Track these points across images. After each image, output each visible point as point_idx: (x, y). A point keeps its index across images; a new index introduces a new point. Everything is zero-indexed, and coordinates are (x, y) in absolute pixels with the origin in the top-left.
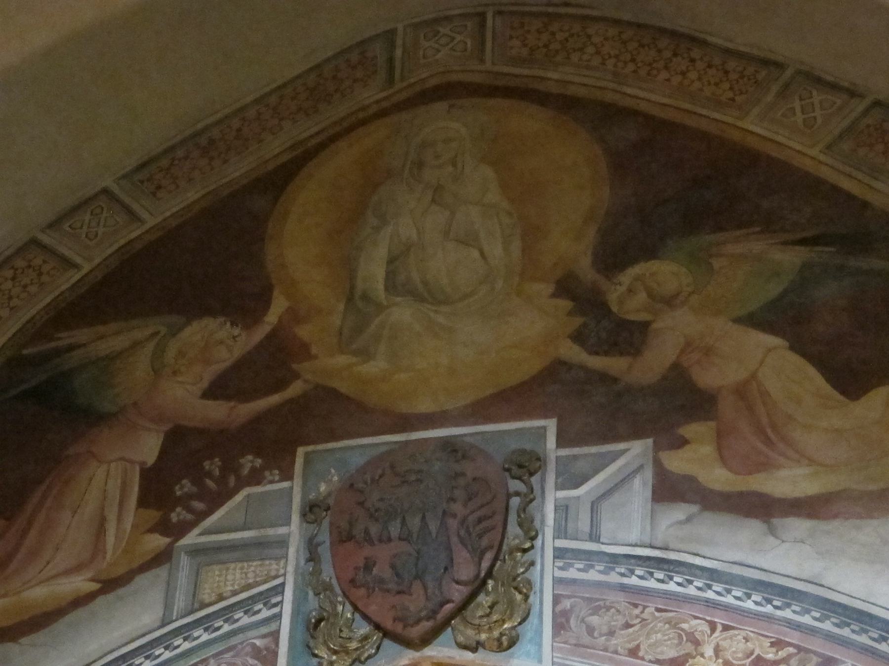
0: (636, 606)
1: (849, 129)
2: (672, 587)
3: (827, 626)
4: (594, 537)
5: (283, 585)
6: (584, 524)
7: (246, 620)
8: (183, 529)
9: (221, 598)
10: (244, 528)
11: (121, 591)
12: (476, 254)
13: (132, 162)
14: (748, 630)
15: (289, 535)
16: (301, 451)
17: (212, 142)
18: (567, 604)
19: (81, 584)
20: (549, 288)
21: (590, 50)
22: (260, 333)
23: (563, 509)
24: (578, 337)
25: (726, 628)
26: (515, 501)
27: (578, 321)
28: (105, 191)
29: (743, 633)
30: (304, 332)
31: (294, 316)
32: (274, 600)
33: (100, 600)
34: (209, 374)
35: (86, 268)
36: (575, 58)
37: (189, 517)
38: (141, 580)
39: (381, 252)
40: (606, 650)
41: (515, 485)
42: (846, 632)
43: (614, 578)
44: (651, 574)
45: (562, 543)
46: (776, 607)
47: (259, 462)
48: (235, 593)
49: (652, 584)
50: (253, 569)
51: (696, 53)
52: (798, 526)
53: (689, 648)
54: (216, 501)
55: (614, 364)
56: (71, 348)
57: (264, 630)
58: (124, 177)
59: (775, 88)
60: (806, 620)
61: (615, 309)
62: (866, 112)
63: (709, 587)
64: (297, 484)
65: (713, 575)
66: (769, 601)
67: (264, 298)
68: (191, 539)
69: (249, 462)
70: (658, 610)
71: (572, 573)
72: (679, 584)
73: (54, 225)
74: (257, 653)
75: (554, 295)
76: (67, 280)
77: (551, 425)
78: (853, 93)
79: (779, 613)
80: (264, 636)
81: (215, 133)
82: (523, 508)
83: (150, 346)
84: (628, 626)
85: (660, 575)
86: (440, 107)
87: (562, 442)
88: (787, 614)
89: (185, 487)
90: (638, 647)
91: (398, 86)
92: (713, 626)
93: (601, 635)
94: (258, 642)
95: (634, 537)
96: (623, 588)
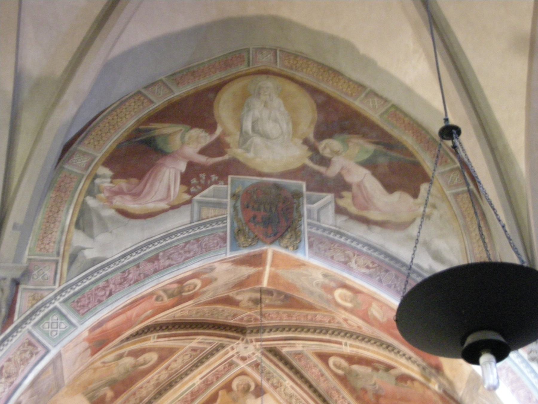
1: (386, 111)
6: (315, 216)
8: (194, 194)
13: (169, 74)
17: (194, 72)
18: (312, 239)
19: (163, 205)
20: (301, 142)
23: (309, 211)
24: (311, 158)
28: (161, 80)
30: (228, 139)
32: (225, 221)
36: (305, 70)
38: (183, 208)
41: (295, 201)
45: (309, 221)
47: (217, 178)
48: (212, 217)
50: (217, 211)
52: (377, 229)
53: (347, 259)
54: (205, 187)
55: (322, 169)
56: (155, 129)
57: (222, 230)
61: (321, 152)
64: (229, 186)
65: (354, 239)
68: (198, 197)
69: (214, 177)
73: (147, 87)
74: (220, 237)
76: (152, 107)
77: (304, 185)
78: (386, 101)
80: (223, 232)
81: (195, 69)
86: (264, 77)
87: (308, 189)
91: (251, 67)
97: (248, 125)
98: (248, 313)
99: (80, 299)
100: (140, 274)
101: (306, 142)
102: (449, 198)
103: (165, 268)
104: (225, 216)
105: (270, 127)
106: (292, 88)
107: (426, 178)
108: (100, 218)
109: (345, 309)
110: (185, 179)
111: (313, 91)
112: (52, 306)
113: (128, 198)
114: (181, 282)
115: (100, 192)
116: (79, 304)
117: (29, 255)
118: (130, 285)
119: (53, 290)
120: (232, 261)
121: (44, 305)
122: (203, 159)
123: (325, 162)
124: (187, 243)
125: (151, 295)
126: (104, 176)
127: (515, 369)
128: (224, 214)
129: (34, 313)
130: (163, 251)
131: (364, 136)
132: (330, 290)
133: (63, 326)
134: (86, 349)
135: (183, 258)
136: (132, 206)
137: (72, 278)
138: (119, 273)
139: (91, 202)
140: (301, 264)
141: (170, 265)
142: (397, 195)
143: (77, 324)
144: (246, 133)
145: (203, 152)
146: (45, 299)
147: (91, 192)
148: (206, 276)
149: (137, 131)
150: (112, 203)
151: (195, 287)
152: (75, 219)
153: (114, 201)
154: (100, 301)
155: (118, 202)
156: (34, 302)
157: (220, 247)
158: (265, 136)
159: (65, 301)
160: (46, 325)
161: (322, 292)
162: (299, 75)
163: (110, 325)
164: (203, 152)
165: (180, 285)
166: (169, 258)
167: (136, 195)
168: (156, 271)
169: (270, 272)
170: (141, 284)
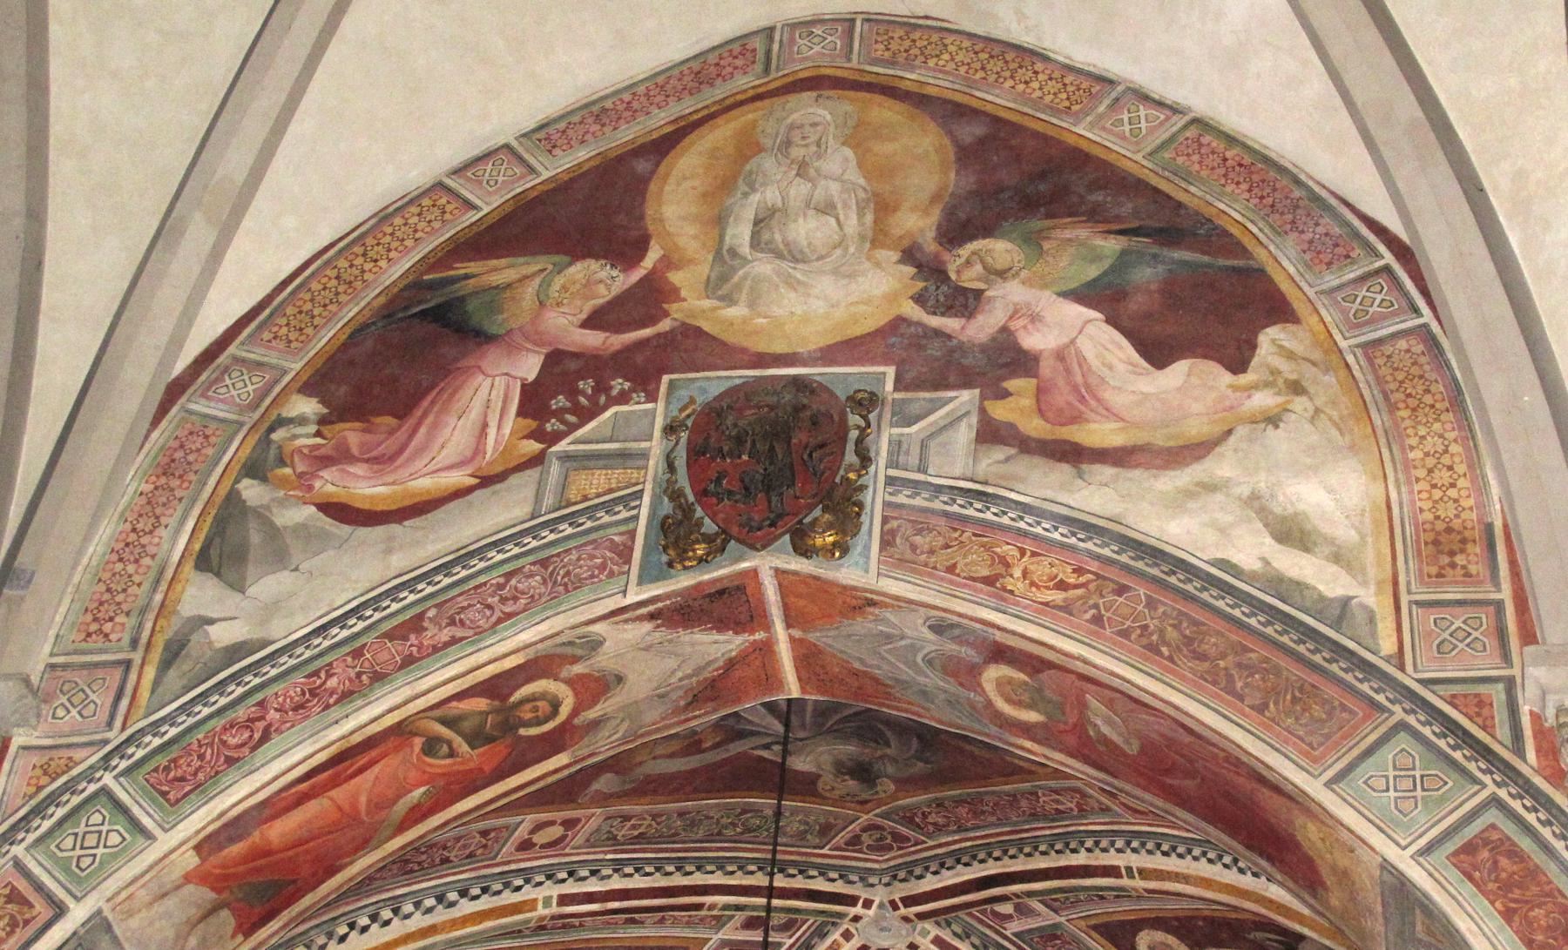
0: (955, 530)
2: (989, 516)
3: (1124, 558)
4: (922, 469)
5: (642, 491)
6: (914, 460)
7: (607, 519)
8: (556, 437)
9: (586, 498)
10: (611, 440)
11: (498, 487)
12: (832, 221)
13: (531, 124)
14: (1053, 557)
15: (650, 448)
16: (666, 378)
17: (604, 110)
18: (895, 524)
19: (460, 478)
20: (894, 256)
21: (946, 57)
22: (636, 275)
23: (897, 445)
24: (919, 299)
25: (1034, 554)
26: (854, 434)
27: (921, 285)
28: (507, 147)
29: (1050, 560)
30: (675, 277)
31: (667, 263)
32: (633, 504)
33: (477, 493)
34: (589, 307)
35: (486, 210)
36: (931, 63)
37: (562, 427)
38: (514, 480)
39: (749, 214)
40: (926, 565)
42: (1140, 565)
43: (937, 505)
44: (971, 504)
46: (1079, 539)
47: (627, 385)
48: (598, 495)
49: (970, 512)
50: (616, 476)
51: (1039, 66)
52: (1106, 471)
53: (1000, 569)
55: (951, 324)
56: (467, 277)
57: (623, 528)
58: (524, 135)
59: (1107, 102)
60: (1106, 552)
61: (953, 276)
62: (1185, 127)
63: (1022, 518)
64: (661, 406)
65: (1026, 509)
66: (1074, 534)
67: (641, 246)
68: (562, 446)
69: (619, 385)
70: (975, 535)
71: (901, 499)
72: (995, 514)
73: (458, 172)
74: (614, 547)
75: (900, 262)
77: (890, 371)
78: (1175, 110)
79: (1081, 544)
80: (621, 534)
81: (608, 104)
82: (859, 442)
83: (538, 281)
84: (947, 546)
85: (979, 505)
86: (808, 96)
88: (1089, 545)
89: (560, 401)
90: (954, 566)
91: (773, 75)
92: (1022, 552)
93: (922, 553)
94: (616, 538)
95: (957, 472)
96: (946, 514)
97: (740, 233)
98: (864, 819)
99: (174, 761)
100: (359, 675)
101: (910, 255)
102: (1350, 359)
103: (436, 649)
104: (639, 487)
105: (806, 230)
106: (885, 112)
107: (1279, 310)
108: (273, 533)
109: (1026, 730)
110: (533, 401)
111: (949, 112)
112: (92, 788)
113: (359, 469)
114: (496, 687)
115: (281, 462)
116: (172, 774)
117: (52, 655)
118: (328, 707)
119: (106, 742)
120: (652, 617)
121: (69, 787)
122: (594, 339)
123: (965, 302)
124: (509, 575)
125: (401, 732)
126: (302, 420)
127: (1525, 843)
128: (637, 484)
129: (38, 811)
130: (436, 606)
131: (1094, 216)
132: (968, 674)
133: (114, 839)
134: (214, 910)
135: (498, 614)
136: (365, 488)
137: (163, 707)
138: (299, 678)
139: (252, 491)
140: (861, 603)
141: (454, 641)
142: (1180, 368)
143: (157, 831)
144: (733, 253)
145: (593, 321)
146: (75, 772)
147: (254, 469)
148: (578, 669)
149: (414, 286)
150: (310, 488)
151: (556, 706)
152: (197, 546)
153: (317, 484)
154: (230, 761)
155: (330, 483)
156: (44, 780)
157: (611, 574)
158: (793, 255)
159: (128, 772)
160: (69, 842)
161: (951, 686)
162: (912, 77)
163: (280, 830)
164: (593, 321)
165: (496, 703)
166: (452, 623)
167: (382, 462)
168: (408, 661)
169: (792, 639)
170: (360, 702)
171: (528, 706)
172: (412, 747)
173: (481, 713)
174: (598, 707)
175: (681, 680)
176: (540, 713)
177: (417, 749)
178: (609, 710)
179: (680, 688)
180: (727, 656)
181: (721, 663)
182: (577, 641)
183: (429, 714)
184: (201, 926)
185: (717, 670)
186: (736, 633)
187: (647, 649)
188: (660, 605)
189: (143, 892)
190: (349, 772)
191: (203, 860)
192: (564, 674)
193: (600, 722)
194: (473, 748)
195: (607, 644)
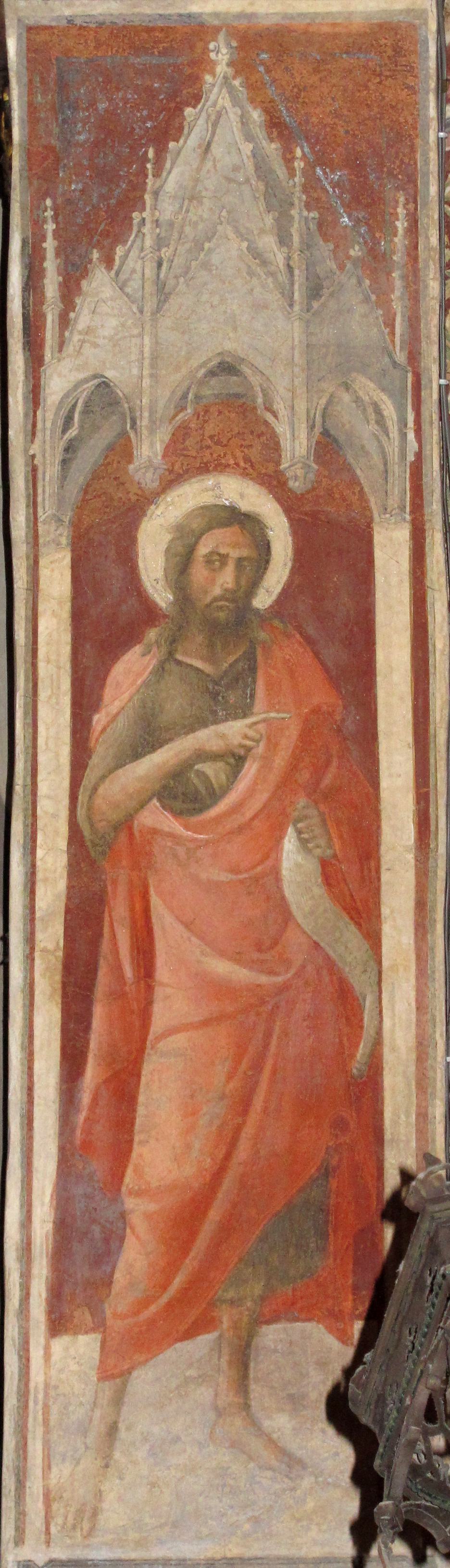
165: (152, 634)
171: (199, 573)
172: (155, 831)
173: (160, 670)
174: (282, 429)
175: (284, 240)
176: (235, 554)
177: (169, 823)
178: (301, 407)
179: (307, 246)
180: (260, 134)
181: (272, 149)
182: (73, 432)
183: (90, 776)
184: (255, 1389)
185: (288, 161)
186: (196, 99)
187: (163, 293)
188: (50, 245)
189: (60, 1473)
190: (128, 971)
191: (99, 1325)
192: (149, 480)
193: (326, 433)
194: (244, 711)
195: (110, 374)
